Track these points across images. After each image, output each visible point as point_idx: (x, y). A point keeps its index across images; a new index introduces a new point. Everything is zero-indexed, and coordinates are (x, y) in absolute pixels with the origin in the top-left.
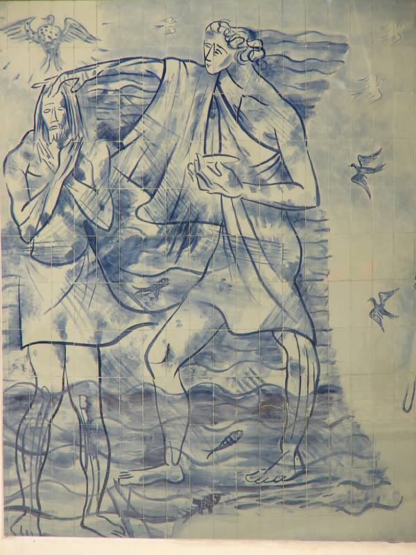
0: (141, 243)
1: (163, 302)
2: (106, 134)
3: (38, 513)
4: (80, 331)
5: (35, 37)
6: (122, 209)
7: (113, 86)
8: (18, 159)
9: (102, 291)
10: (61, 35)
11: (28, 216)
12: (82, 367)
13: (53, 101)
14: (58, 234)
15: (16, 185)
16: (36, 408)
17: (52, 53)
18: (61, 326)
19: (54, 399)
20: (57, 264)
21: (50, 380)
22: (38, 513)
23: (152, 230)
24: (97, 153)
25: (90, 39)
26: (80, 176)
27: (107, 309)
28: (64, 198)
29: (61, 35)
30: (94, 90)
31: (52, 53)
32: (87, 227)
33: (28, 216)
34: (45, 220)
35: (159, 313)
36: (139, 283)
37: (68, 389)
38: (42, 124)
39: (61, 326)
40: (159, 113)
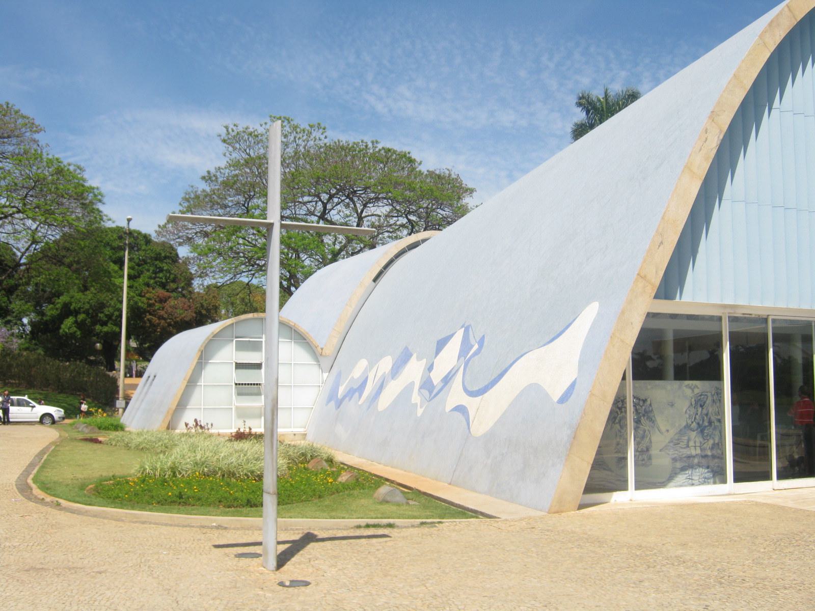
0: (706, 427)
1: (709, 438)
2: (701, 406)
3: (692, 479)
4: (698, 444)
5: (690, 388)
6: (703, 421)
7: (702, 397)
8: (688, 411)
9: (701, 436)
10: (694, 388)
11: (689, 422)
12: (698, 451)
13: (693, 400)
14: (694, 425)
15: (687, 416)
16: (692, 459)
17: (693, 391)
18: (695, 442)
19: (694, 457)
20: (694, 431)
21: (693, 452)
22: (692, 479)
24: (700, 409)
25: (698, 388)
26: (697, 414)
27: (701, 440)
28: (695, 418)
29: (694, 388)
30: (699, 398)
31: (693, 391)
32: (698, 424)
33: (689, 422)
34: (692, 422)
35: (708, 440)
36: (705, 434)
37: (696, 455)
40: (707, 402)
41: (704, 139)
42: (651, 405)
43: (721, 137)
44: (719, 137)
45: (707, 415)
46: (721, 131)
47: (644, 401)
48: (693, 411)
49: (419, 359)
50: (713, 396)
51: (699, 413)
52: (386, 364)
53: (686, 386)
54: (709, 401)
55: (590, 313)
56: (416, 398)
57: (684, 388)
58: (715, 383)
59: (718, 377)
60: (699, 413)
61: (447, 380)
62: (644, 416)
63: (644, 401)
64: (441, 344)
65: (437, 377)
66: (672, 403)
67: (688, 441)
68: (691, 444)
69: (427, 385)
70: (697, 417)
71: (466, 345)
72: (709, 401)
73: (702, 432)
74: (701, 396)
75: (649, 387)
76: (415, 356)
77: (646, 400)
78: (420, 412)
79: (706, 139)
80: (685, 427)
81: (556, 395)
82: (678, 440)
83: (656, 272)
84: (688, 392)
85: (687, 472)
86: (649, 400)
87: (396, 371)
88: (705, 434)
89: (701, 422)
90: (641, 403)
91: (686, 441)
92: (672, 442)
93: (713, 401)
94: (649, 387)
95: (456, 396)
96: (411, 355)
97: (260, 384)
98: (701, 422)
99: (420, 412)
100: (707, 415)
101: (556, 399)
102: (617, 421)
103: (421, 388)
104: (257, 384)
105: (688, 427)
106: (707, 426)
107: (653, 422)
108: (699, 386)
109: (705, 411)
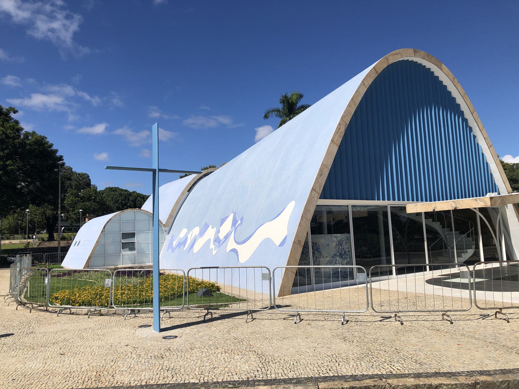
2: (341, 245)
5: (336, 237)
6: (342, 252)
13: (337, 242)
15: (335, 250)
17: (337, 238)
18: (339, 262)
20: (338, 256)
23: (344, 253)
24: (340, 247)
27: (342, 260)
28: (339, 251)
31: (337, 238)
32: (340, 253)
34: (337, 253)
36: (343, 258)
38: (337, 245)
39: (339, 262)
41: (339, 128)
42: (319, 245)
43: (346, 127)
44: (345, 127)
45: (343, 249)
46: (346, 124)
47: (316, 244)
48: (338, 247)
49: (212, 228)
50: (346, 240)
51: (340, 249)
52: (196, 231)
53: (334, 237)
54: (344, 243)
55: (291, 206)
56: (212, 246)
57: (333, 237)
58: (346, 235)
59: (349, 232)
60: (340, 249)
61: (227, 237)
62: (316, 250)
63: (316, 244)
64: (223, 221)
65: (222, 236)
66: (328, 244)
67: (336, 260)
68: (337, 262)
69: (217, 240)
70: (339, 250)
71: (235, 222)
72: (344, 243)
73: (342, 257)
74: (341, 240)
75: (318, 238)
76: (210, 226)
77: (317, 243)
78: (214, 252)
79: (340, 128)
80: (334, 255)
81: (278, 242)
82: (332, 260)
83: (320, 187)
84: (334, 239)
85: (336, 275)
86: (318, 243)
87: (202, 233)
88: (343, 258)
89: (341, 253)
90: (315, 245)
91: (335, 261)
92: (329, 262)
93: (346, 243)
94: (318, 238)
95: (231, 244)
96: (209, 226)
97: (134, 243)
98: (341, 253)
99: (214, 252)
100: (343, 249)
101: (278, 245)
102: (304, 253)
103: (215, 241)
104: (133, 243)
105: (335, 255)
106: (344, 254)
107: (320, 253)
108: (339, 237)
109: (342, 247)
